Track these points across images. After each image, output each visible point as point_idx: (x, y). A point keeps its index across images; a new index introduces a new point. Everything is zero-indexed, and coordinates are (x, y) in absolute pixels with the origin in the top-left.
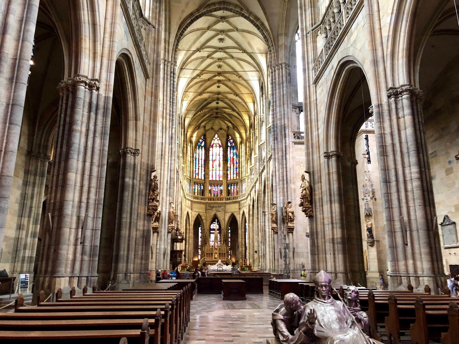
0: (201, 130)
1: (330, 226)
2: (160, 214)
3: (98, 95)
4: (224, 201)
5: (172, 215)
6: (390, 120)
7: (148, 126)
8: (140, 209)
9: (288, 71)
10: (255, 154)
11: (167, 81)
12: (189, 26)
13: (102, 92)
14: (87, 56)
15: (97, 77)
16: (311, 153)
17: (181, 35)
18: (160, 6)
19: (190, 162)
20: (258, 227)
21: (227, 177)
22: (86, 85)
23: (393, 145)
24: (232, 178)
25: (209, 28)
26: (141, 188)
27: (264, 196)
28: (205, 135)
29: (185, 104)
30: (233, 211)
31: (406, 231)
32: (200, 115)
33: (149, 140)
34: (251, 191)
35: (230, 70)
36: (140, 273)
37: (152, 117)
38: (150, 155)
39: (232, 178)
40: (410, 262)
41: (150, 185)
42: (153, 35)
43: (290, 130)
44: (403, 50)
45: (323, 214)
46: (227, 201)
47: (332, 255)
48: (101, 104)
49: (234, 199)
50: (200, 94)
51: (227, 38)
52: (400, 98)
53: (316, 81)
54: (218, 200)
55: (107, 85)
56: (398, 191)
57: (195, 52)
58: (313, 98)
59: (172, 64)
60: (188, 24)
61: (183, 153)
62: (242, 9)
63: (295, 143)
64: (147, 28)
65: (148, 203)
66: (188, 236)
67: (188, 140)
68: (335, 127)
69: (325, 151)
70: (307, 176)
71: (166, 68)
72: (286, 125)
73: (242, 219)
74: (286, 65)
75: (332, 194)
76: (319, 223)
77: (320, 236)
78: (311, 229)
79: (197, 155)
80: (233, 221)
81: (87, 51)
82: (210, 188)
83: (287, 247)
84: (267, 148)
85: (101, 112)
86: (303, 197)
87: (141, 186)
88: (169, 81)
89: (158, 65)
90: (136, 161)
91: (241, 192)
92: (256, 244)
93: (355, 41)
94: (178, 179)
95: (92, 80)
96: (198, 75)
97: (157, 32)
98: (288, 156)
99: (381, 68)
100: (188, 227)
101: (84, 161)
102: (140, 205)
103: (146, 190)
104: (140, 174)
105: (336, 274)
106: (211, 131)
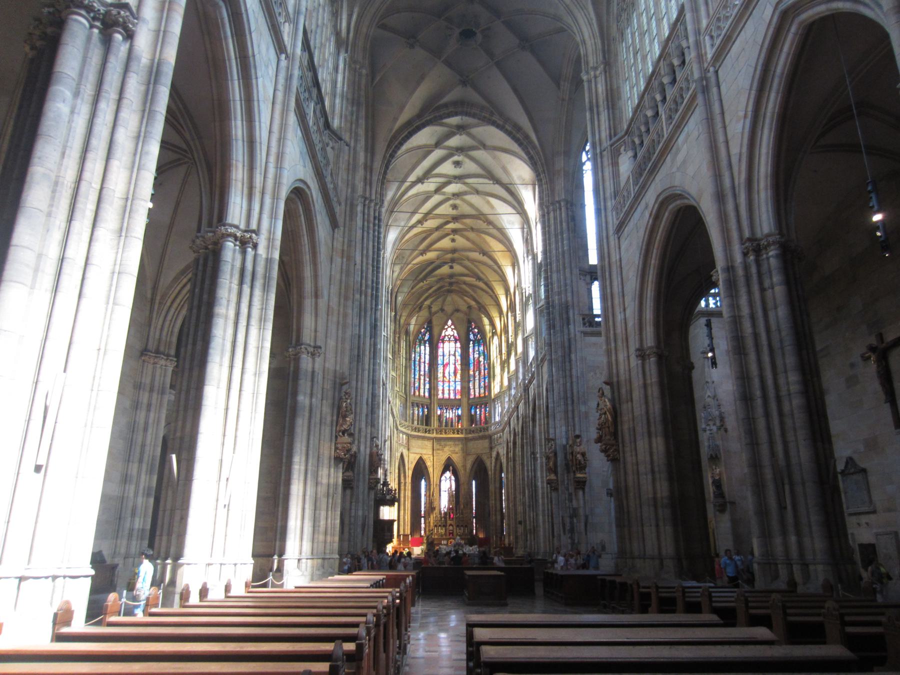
0: (424, 313)
1: (650, 477)
2: (355, 456)
6: (750, 293)
7: (336, 308)
9: (570, 213)
10: (516, 354)
11: (368, 233)
13: (262, 250)
14: (239, 193)
15: (254, 226)
16: (613, 352)
17: (392, 156)
18: (358, 111)
19: (406, 367)
20: (523, 479)
22: (236, 240)
23: (756, 336)
24: (477, 394)
25: (437, 145)
26: (324, 412)
27: (534, 426)
28: (430, 322)
29: (397, 269)
31: (783, 484)
32: (422, 287)
34: (509, 419)
35: (474, 212)
36: (324, 559)
37: (343, 291)
39: (477, 394)
40: (793, 539)
41: (339, 408)
42: (346, 158)
43: (576, 312)
44: (767, 177)
45: (636, 455)
46: (470, 436)
47: (654, 529)
48: (260, 270)
50: (423, 253)
51: (467, 160)
52: (765, 256)
53: (620, 229)
55: (270, 240)
56: (767, 415)
57: (414, 184)
58: (615, 258)
59: (376, 204)
61: (394, 353)
62: (492, 114)
63: (586, 334)
64: (336, 146)
65: (336, 437)
66: (402, 495)
67: (403, 331)
69: (637, 346)
70: (607, 390)
71: (366, 211)
72: (570, 303)
73: (495, 466)
74: (567, 202)
75: (652, 420)
76: (630, 471)
77: (631, 495)
78: (617, 482)
79: (417, 355)
81: (240, 185)
82: (439, 412)
83: (574, 514)
84: (536, 343)
86: (600, 428)
87: (324, 409)
88: (371, 232)
89: (353, 206)
90: (317, 366)
92: (520, 509)
93: (684, 162)
94: (385, 396)
95: (246, 231)
96: (420, 222)
98: (573, 356)
99: (730, 206)
100: (402, 481)
101: (231, 367)
102: (322, 442)
103: (332, 416)
105: (661, 560)
106: (440, 314)
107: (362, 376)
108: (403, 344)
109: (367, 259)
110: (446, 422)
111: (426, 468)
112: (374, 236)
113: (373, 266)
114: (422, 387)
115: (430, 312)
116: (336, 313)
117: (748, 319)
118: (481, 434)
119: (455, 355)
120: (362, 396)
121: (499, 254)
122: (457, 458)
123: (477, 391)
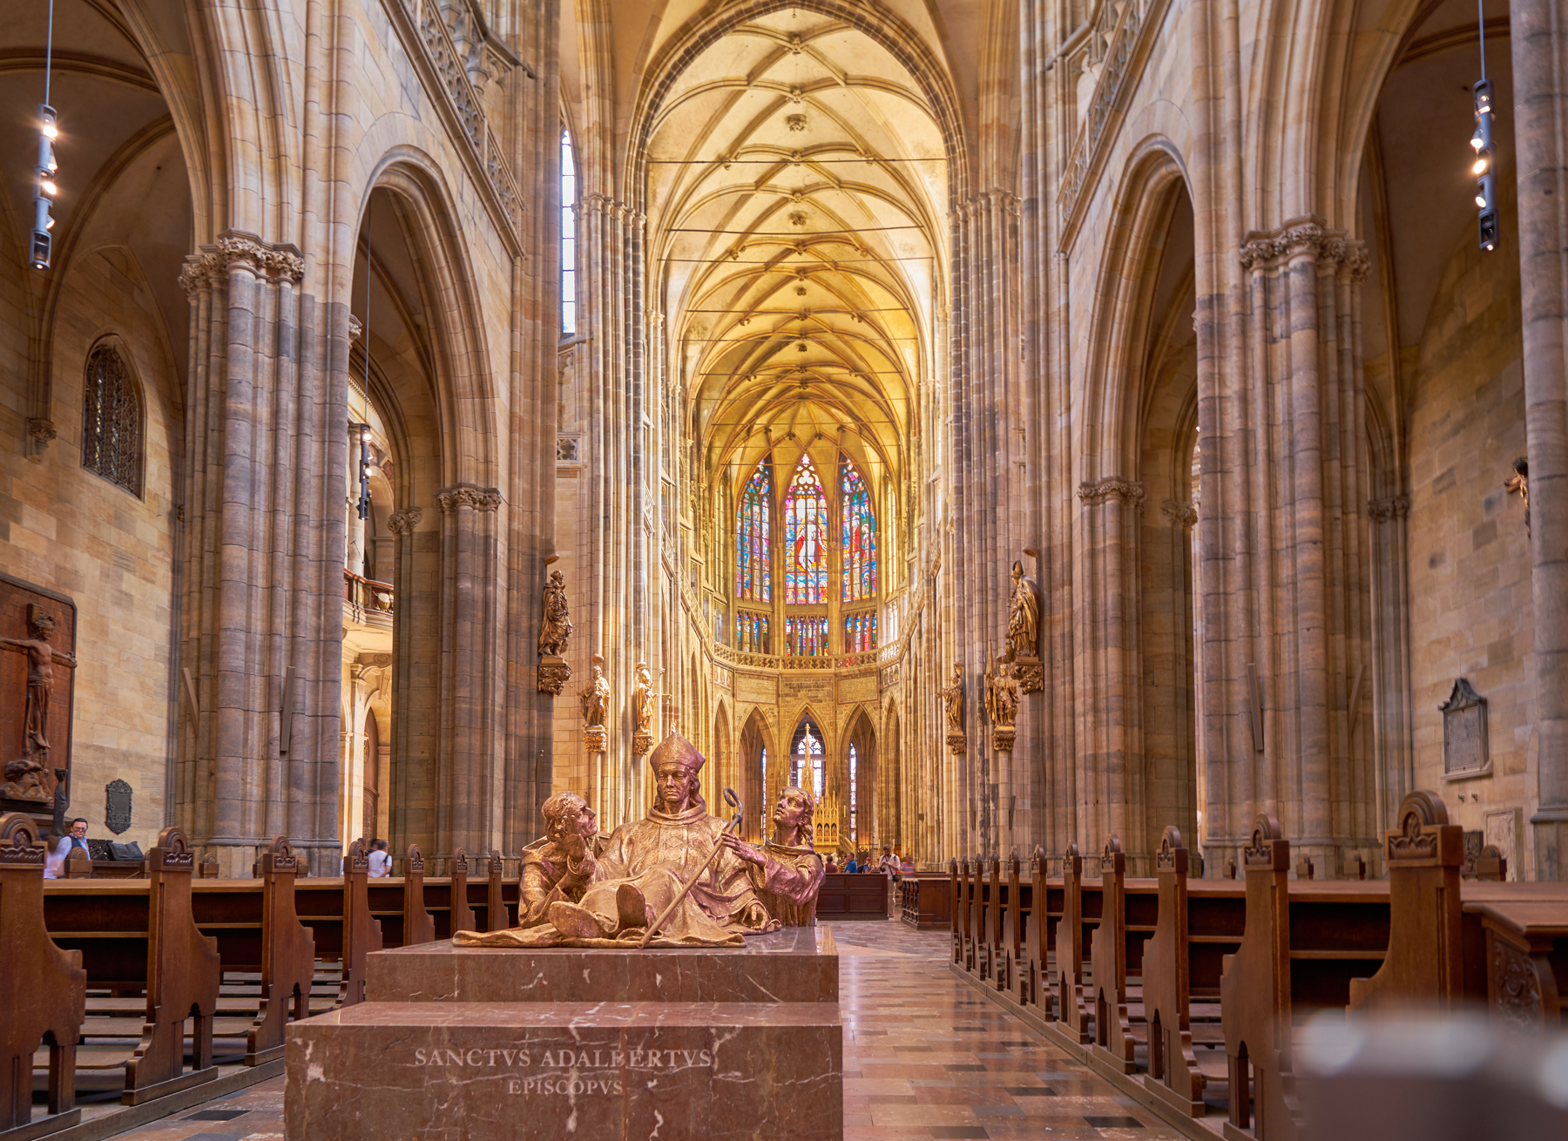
3: (301, 299)
4: (832, 670)
7: (526, 418)
11: (615, 274)
12: (680, 72)
13: (313, 287)
16: (1044, 490)
17: (654, 106)
21: (843, 595)
23: (1246, 433)
24: (857, 595)
28: (769, 459)
32: (748, 390)
33: (532, 460)
37: (539, 385)
39: (857, 595)
42: (531, 104)
43: (1012, 425)
52: (1281, 269)
54: (814, 666)
55: (330, 267)
59: (628, 212)
60: (675, 67)
68: (1118, 398)
72: (1000, 409)
80: (862, 732)
85: (314, 353)
88: (621, 271)
96: (731, 253)
97: (542, 91)
98: (1000, 511)
106: (787, 443)
108: (718, 502)
109: (616, 329)
112: (626, 281)
113: (627, 343)
114: (757, 582)
115: (768, 440)
116: (527, 429)
117: (1236, 403)
118: (863, 667)
119: (816, 523)
121: (888, 316)
123: (857, 588)
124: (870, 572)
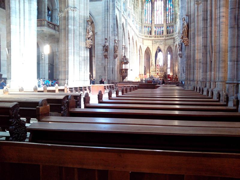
2: (108, 47)
4: (164, 38)
5: (116, 48)
8: (80, 44)
19: (142, 12)
21: (167, 22)
26: (80, 31)
30: (170, 44)
38: (85, 10)
39: (170, 22)
41: (86, 29)
46: (167, 38)
49: (170, 36)
54: (160, 37)
65: (86, 40)
73: (175, 49)
76: (191, 50)
87: (80, 30)
91: (175, 31)
102: (80, 42)
104: (79, 23)
107: (109, 17)
110: (158, 33)
111: (150, 51)
118: (171, 37)
120: (110, 24)
122: (162, 47)
124: (173, 17)
